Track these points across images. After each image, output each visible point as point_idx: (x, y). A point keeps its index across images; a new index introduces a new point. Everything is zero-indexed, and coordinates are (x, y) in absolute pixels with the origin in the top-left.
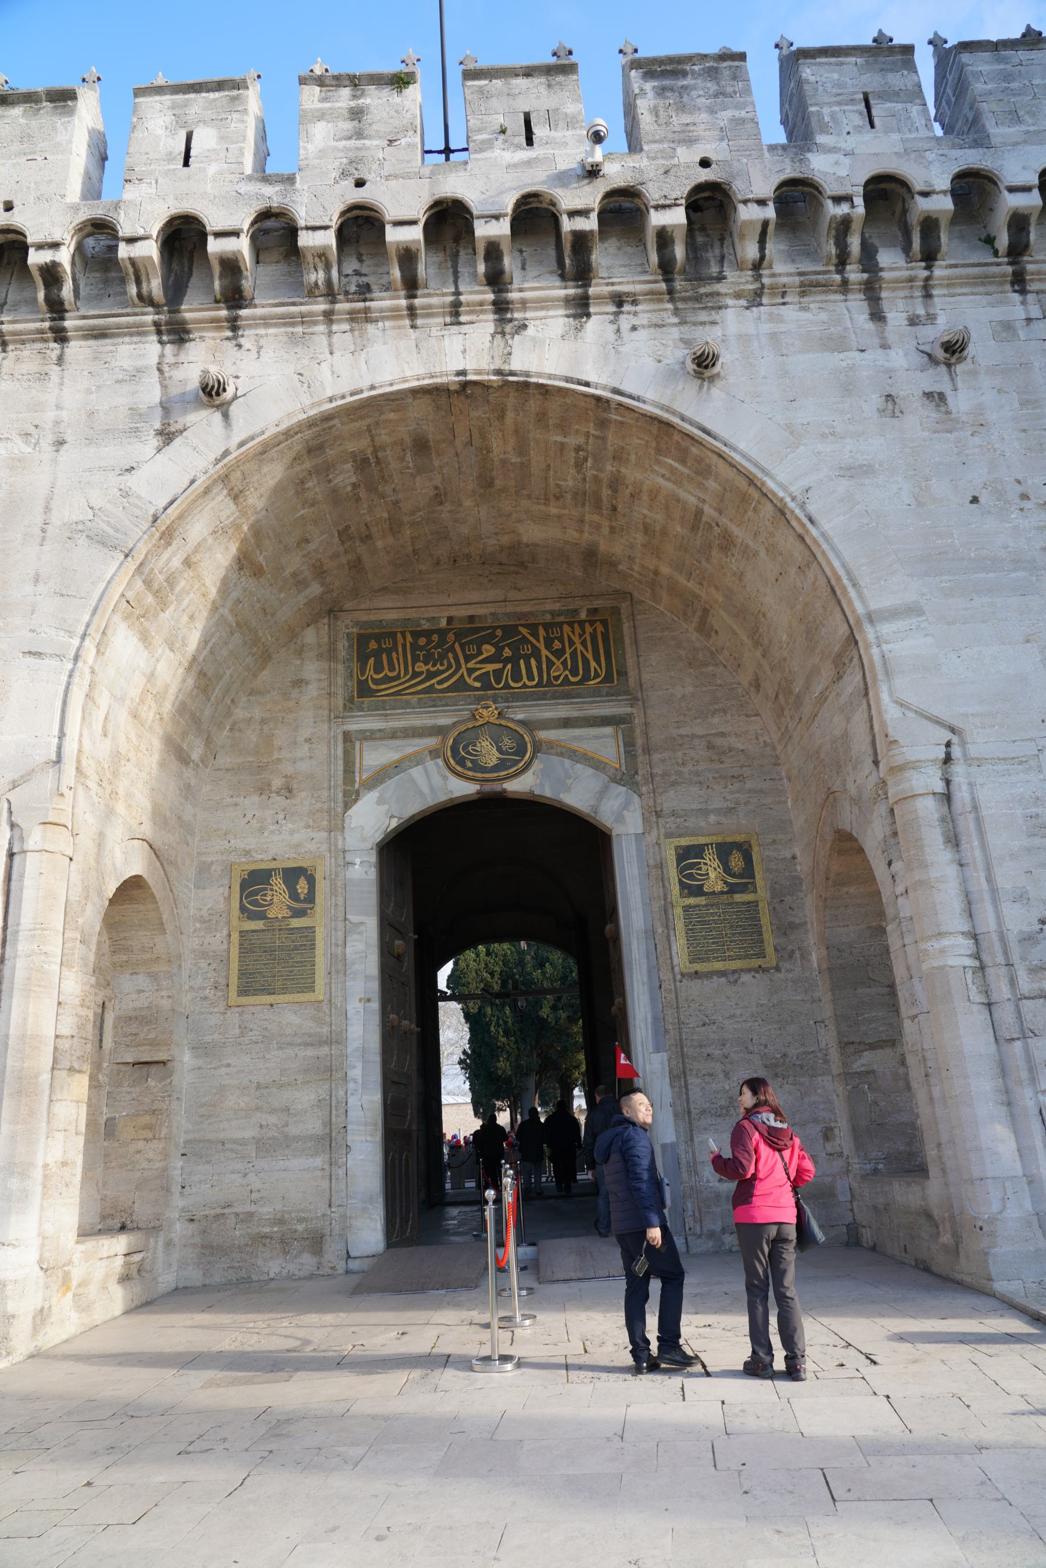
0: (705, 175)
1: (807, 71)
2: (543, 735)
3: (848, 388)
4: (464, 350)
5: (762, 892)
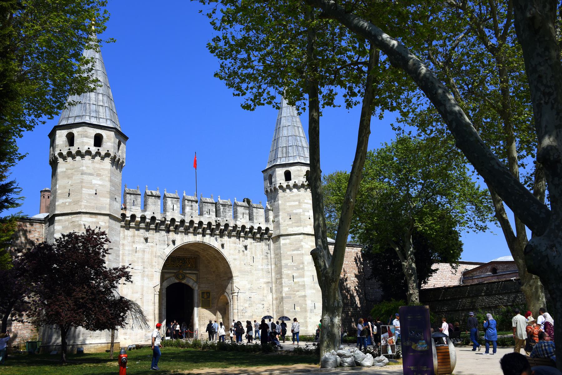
0: (227, 222)
1: (239, 208)
2: (187, 275)
3: (235, 249)
4: (199, 238)
5: (211, 299)
